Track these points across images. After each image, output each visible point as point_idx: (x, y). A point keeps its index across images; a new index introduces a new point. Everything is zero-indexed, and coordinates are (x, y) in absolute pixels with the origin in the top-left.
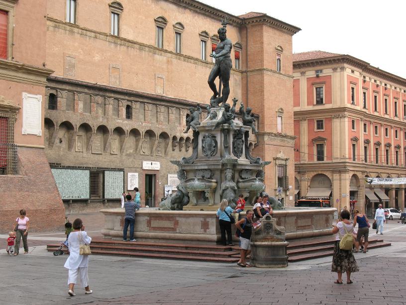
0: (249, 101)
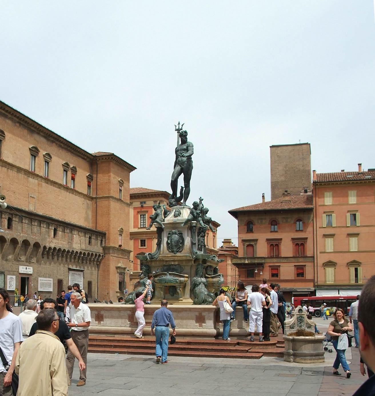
0: (97, 221)
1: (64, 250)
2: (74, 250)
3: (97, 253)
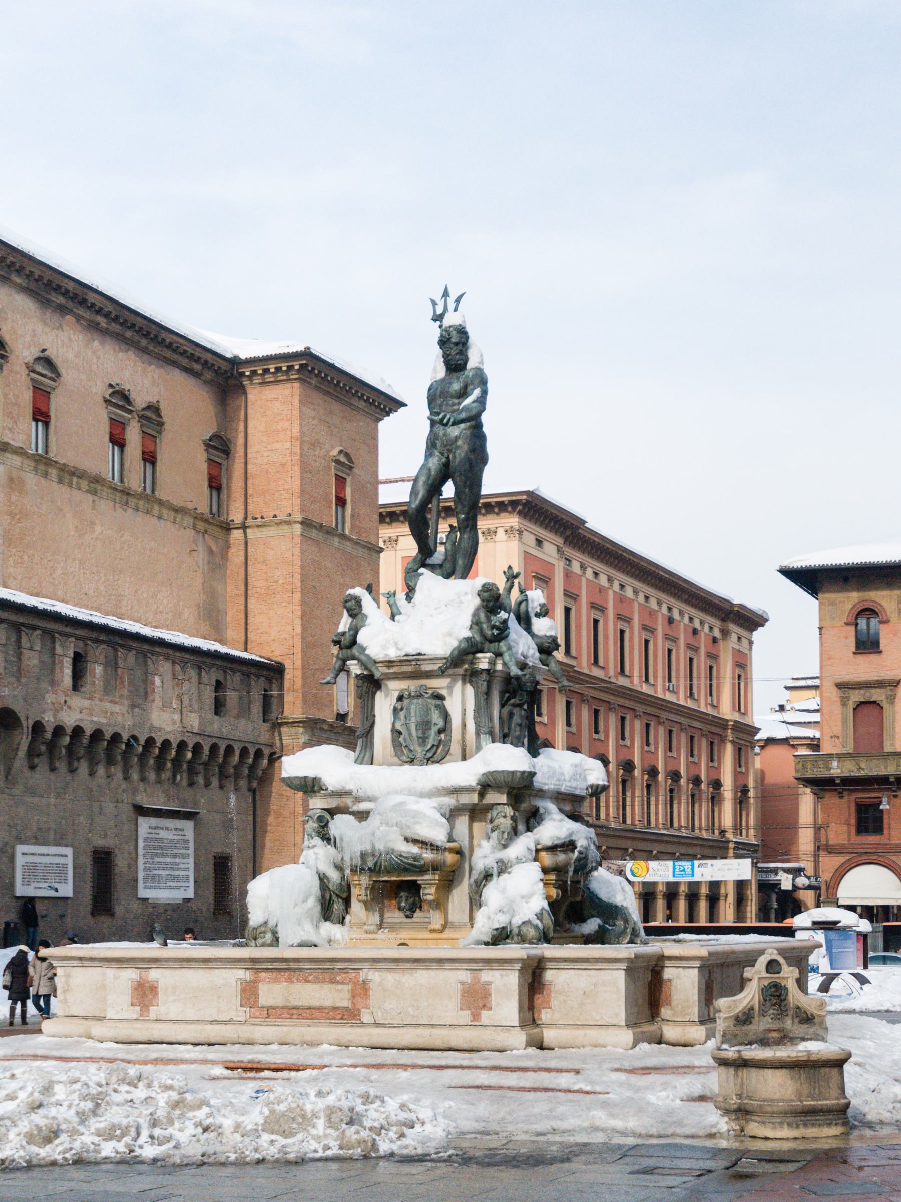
1: (116, 737)
2: (153, 735)
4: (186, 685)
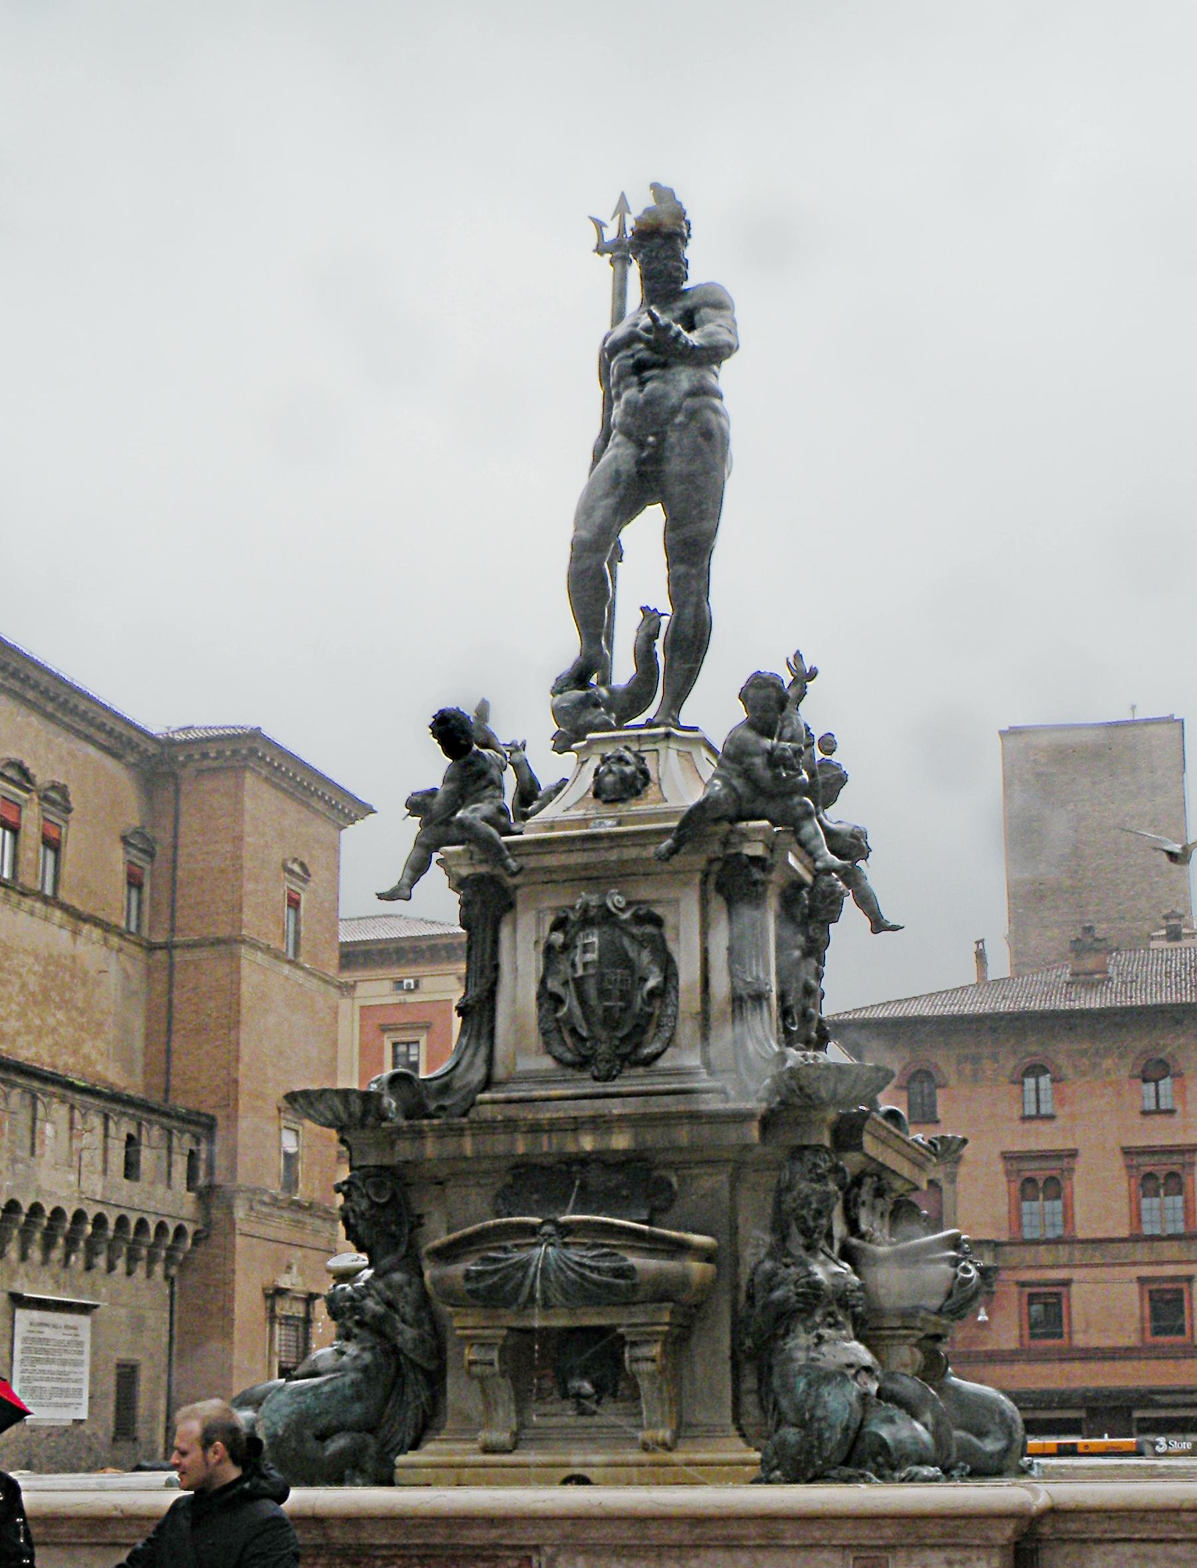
2: (40, 1201)
3: (167, 1220)
4: (87, 1139)
